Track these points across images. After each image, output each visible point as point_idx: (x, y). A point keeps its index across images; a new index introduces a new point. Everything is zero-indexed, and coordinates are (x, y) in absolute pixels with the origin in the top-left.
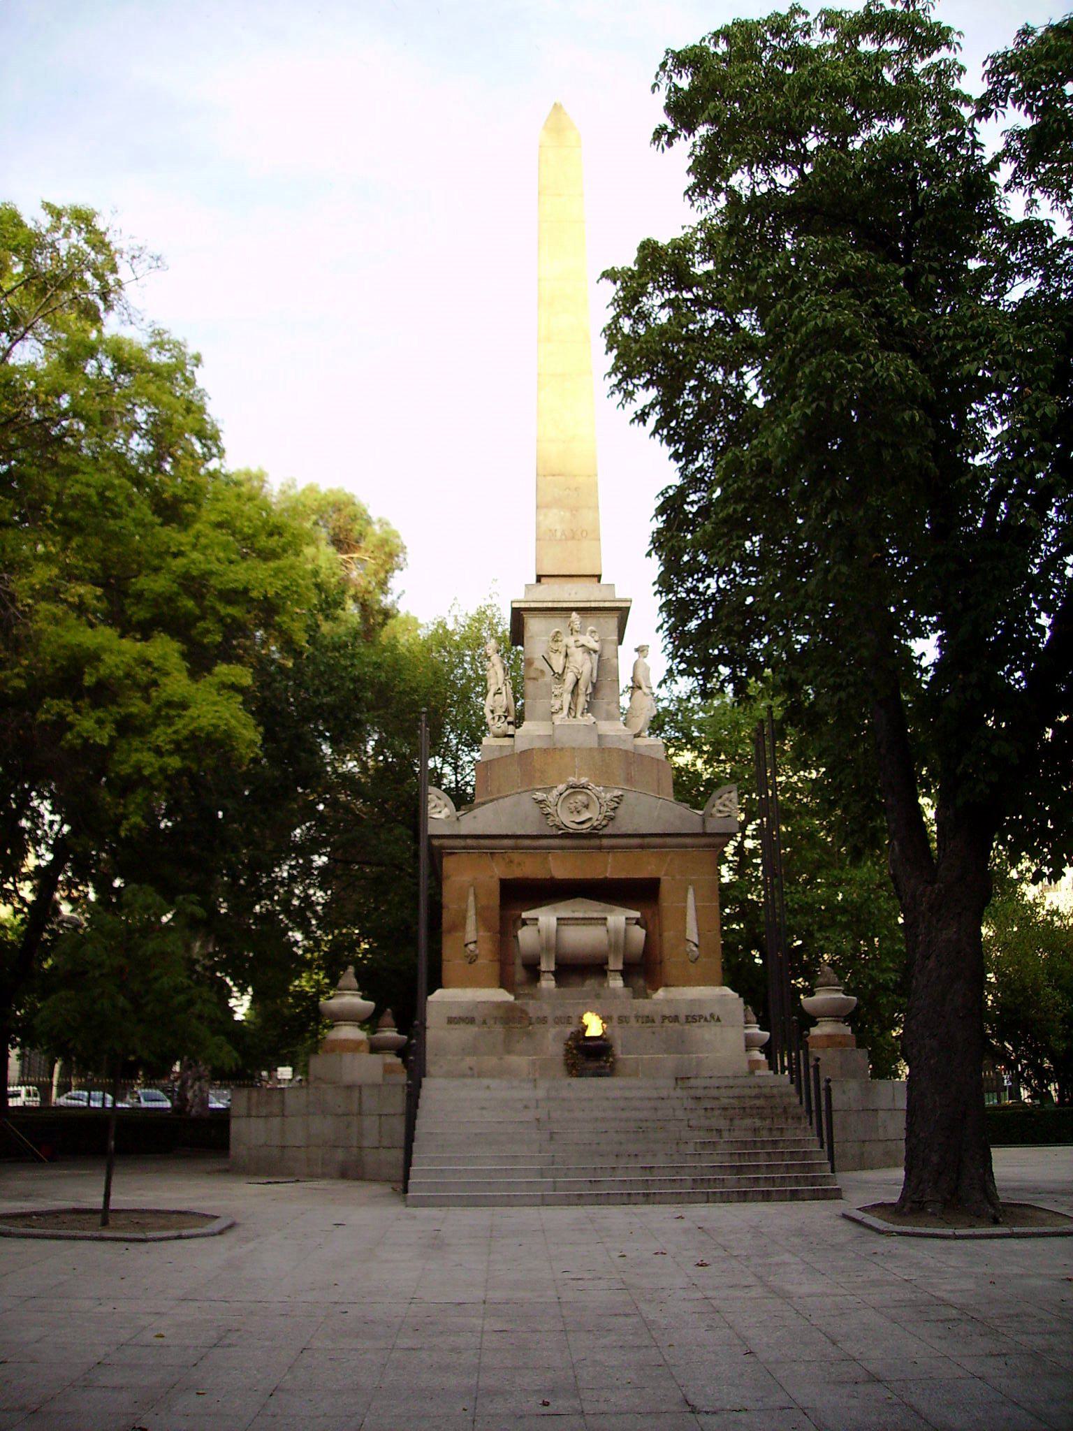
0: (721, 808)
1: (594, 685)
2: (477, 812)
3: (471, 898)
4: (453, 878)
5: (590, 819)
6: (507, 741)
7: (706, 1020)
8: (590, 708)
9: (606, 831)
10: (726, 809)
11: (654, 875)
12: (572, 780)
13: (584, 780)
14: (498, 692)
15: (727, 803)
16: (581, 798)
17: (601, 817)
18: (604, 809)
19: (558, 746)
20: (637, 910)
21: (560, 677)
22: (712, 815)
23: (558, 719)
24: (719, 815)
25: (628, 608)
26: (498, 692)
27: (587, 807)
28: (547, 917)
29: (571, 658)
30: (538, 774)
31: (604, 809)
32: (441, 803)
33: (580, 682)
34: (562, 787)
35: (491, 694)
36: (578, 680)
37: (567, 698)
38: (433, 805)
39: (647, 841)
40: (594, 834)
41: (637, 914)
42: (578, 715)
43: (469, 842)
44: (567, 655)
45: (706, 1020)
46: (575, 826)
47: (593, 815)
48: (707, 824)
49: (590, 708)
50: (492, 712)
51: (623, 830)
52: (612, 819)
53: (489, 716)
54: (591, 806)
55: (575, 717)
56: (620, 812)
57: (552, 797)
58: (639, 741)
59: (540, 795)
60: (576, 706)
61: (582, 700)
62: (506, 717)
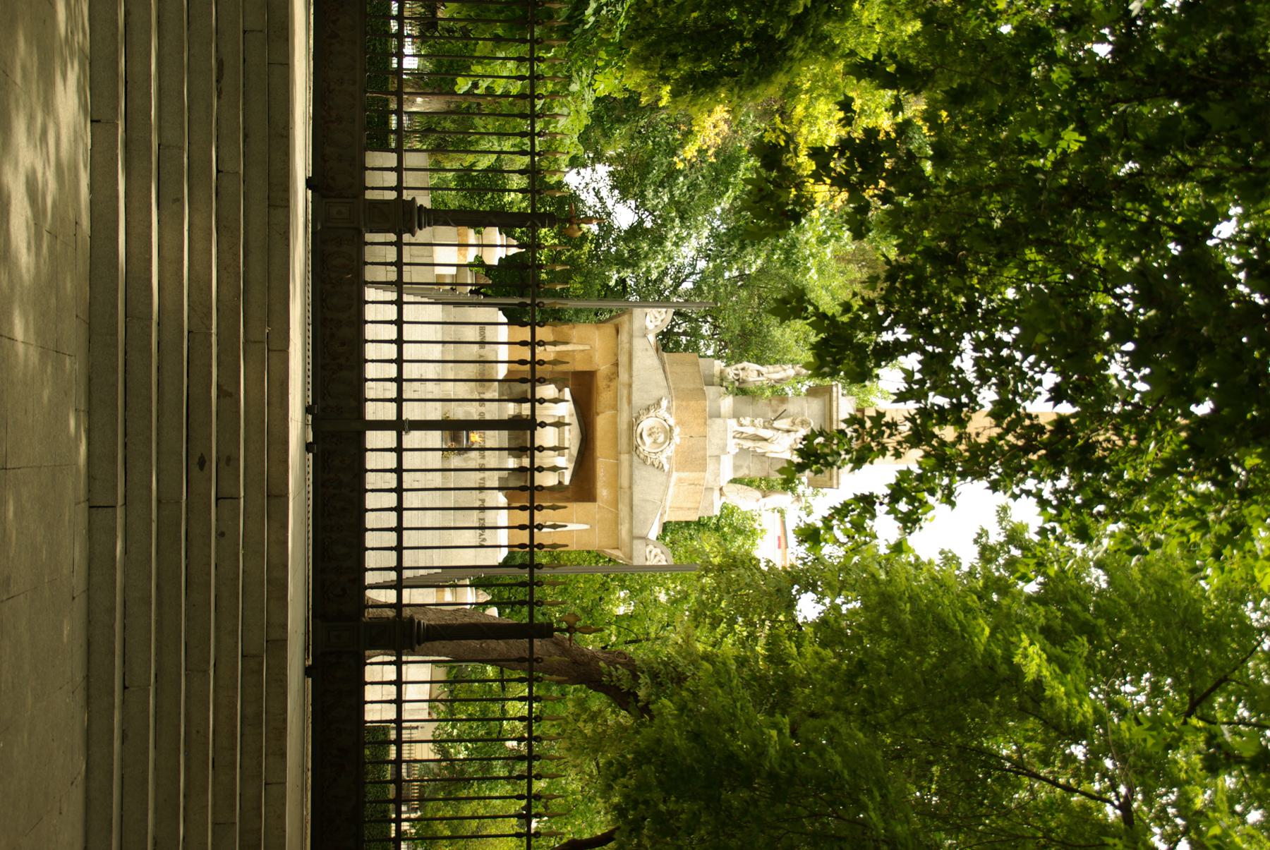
0: (653, 553)
1: (763, 455)
2: (652, 352)
3: (581, 347)
4: (597, 332)
5: (644, 444)
6: (717, 380)
7: (481, 535)
8: (743, 451)
9: (635, 458)
10: (652, 556)
11: (599, 498)
12: (677, 431)
13: (677, 439)
14: (760, 374)
15: (658, 558)
16: (661, 439)
17: (646, 453)
18: (653, 456)
19: (709, 422)
20: (571, 481)
21: (769, 425)
22: (647, 545)
23: (732, 424)
24: (648, 550)
25: (831, 487)
26: (760, 374)
27: (655, 442)
28: (566, 410)
29: (786, 434)
30: (684, 403)
31: (653, 456)
32: (659, 323)
33: (764, 443)
34: (672, 421)
35: (758, 367)
36: (766, 440)
37: (750, 430)
38: (657, 315)
39: (627, 490)
40: (633, 449)
41: (567, 481)
42: (736, 440)
43: (626, 346)
44: (788, 431)
45: (481, 535)
46: (639, 431)
47: (647, 446)
48: (640, 541)
49: (743, 451)
50: (743, 369)
51: (636, 473)
52: (644, 462)
53: (740, 366)
54: (655, 446)
55: (734, 437)
56: (651, 468)
57: (663, 412)
58: (717, 493)
59: (664, 403)
60: (745, 438)
61: (748, 444)
62: (738, 380)
